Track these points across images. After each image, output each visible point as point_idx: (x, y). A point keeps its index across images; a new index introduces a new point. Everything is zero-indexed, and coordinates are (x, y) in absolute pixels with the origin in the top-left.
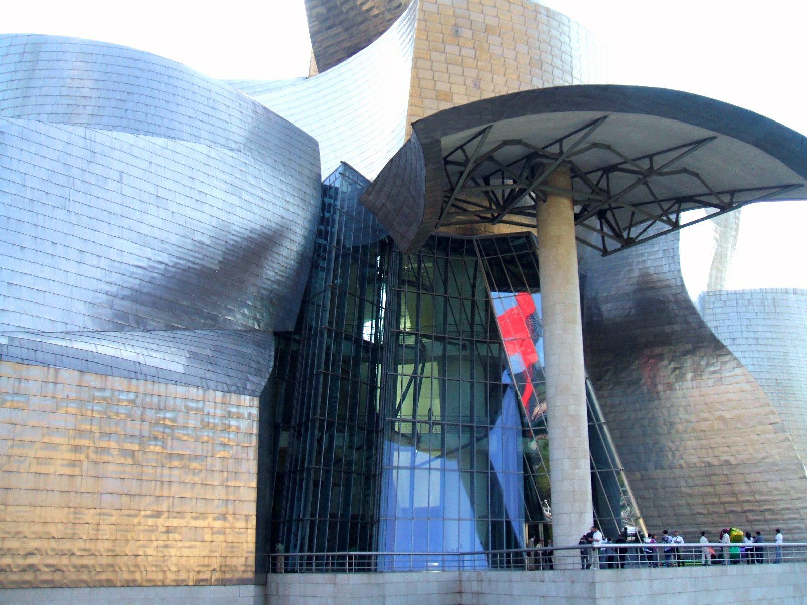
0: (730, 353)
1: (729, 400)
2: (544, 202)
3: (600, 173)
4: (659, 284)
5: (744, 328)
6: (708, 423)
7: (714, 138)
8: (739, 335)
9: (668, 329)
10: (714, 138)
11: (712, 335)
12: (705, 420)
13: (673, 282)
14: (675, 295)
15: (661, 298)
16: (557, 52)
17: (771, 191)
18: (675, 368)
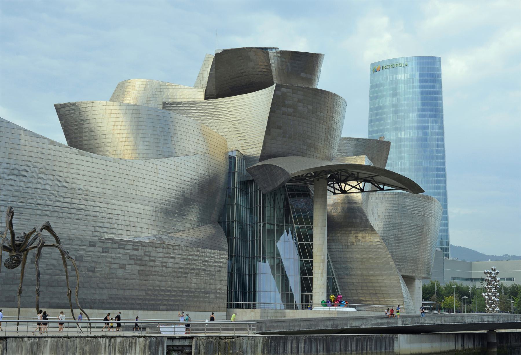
5: (384, 211)
8: (381, 214)
9: (354, 221)
11: (371, 225)
14: (358, 207)
18: (356, 237)
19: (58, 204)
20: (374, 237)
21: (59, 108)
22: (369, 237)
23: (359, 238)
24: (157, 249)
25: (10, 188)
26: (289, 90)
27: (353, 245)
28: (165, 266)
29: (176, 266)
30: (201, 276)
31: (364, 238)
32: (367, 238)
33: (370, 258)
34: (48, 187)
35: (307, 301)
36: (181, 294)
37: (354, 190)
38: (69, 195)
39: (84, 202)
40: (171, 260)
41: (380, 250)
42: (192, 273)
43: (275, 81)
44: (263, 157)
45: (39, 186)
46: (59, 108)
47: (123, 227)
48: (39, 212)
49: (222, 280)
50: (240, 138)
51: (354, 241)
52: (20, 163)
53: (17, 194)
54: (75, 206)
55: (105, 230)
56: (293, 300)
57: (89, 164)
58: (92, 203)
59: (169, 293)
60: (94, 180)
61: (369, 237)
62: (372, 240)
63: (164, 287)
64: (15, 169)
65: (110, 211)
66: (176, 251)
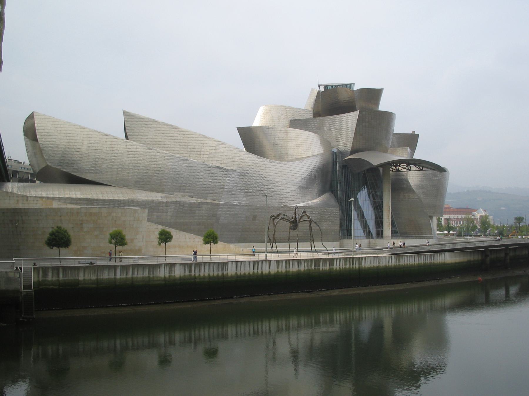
19: (262, 189)
21: (239, 129)
25: (241, 182)
34: (257, 181)
35: (380, 234)
37: (404, 170)
38: (267, 184)
39: (273, 187)
40: (314, 215)
43: (357, 106)
44: (353, 152)
45: (254, 181)
46: (239, 129)
47: (290, 199)
48: (254, 194)
52: (245, 169)
53: (244, 185)
54: (269, 190)
55: (284, 201)
56: (372, 235)
57: (274, 167)
58: (277, 188)
60: (277, 175)
64: (243, 173)
65: (285, 191)
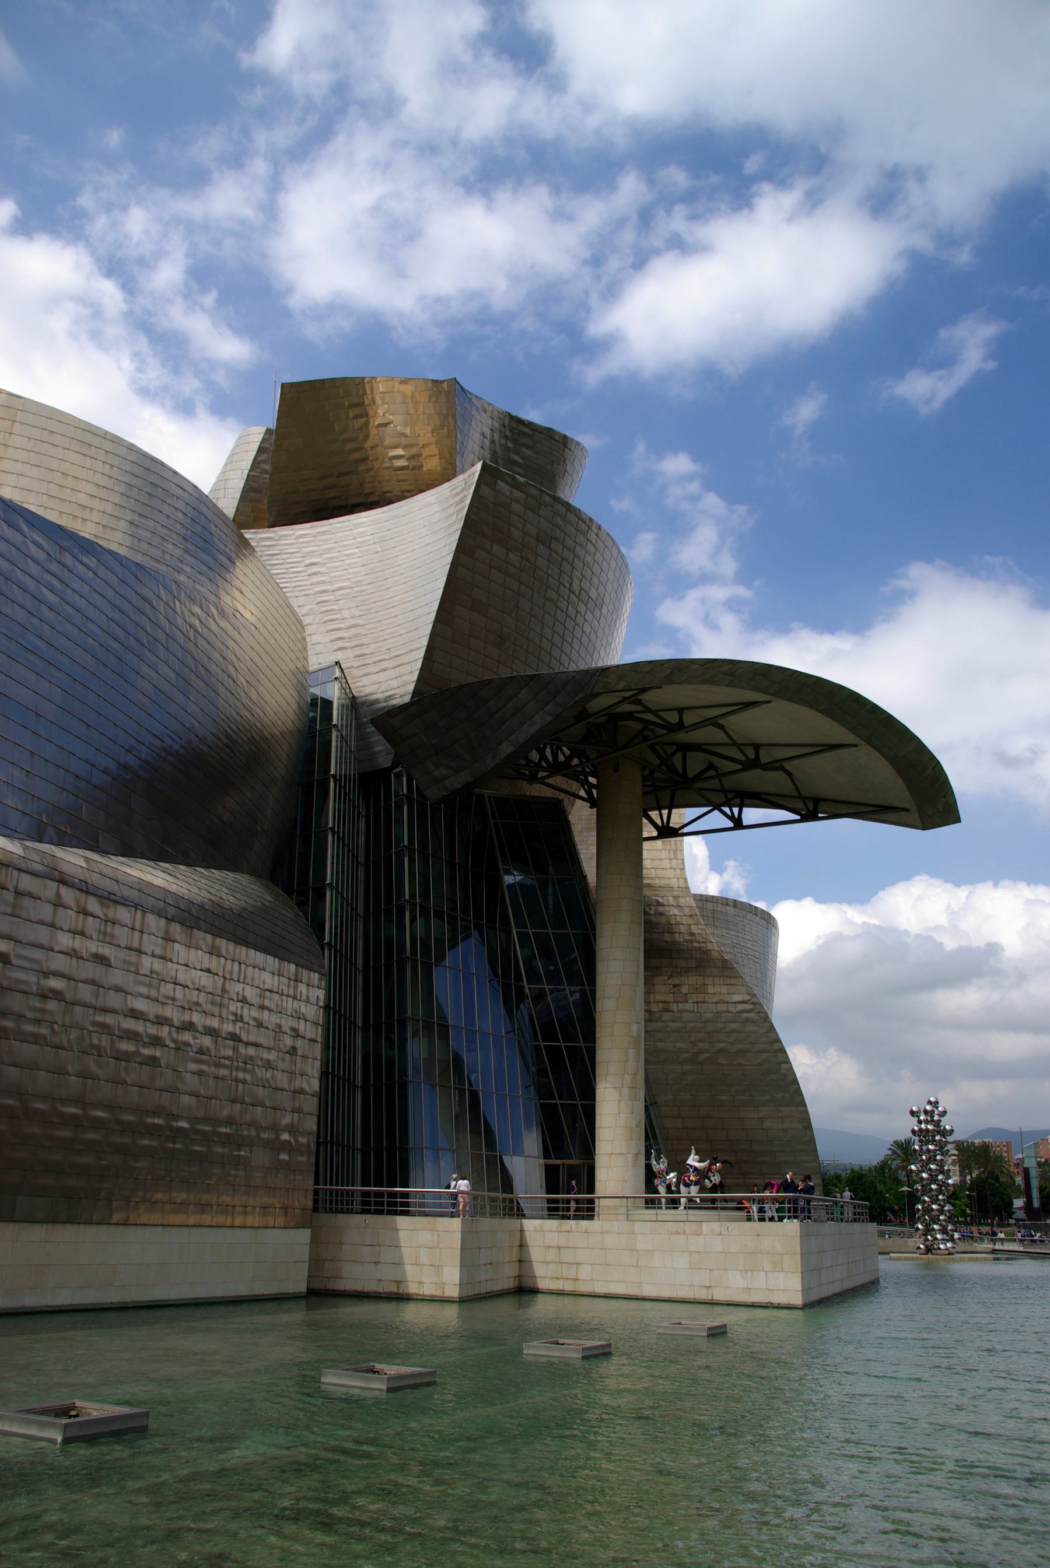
0: (738, 977)
1: (733, 1031)
2: (616, 770)
3: (674, 748)
4: (657, 882)
6: (707, 1055)
7: (855, 746)
10: (855, 746)
12: (701, 1051)
13: (674, 883)
15: (660, 900)
16: (595, 580)
17: (864, 809)
18: (675, 986)
20: (732, 989)
22: (716, 989)
23: (685, 989)
24: (26, 902)
26: (517, 494)
27: (666, 1010)
28: (57, 995)
29: (113, 1000)
30: (218, 1065)
31: (700, 989)
32: (711, 990)
33: (720, 1051)
36: (126, 1140)
40: (90, 970)
41: (750, 1028)
42: (180, 1047)
49: (301, 1091)
50: (340, 644)
51: (670, 997)
59: (66, 1133)
61: (717, 989)
62: (726, 998)
63: (44, 1098)
66: (118, 930)
